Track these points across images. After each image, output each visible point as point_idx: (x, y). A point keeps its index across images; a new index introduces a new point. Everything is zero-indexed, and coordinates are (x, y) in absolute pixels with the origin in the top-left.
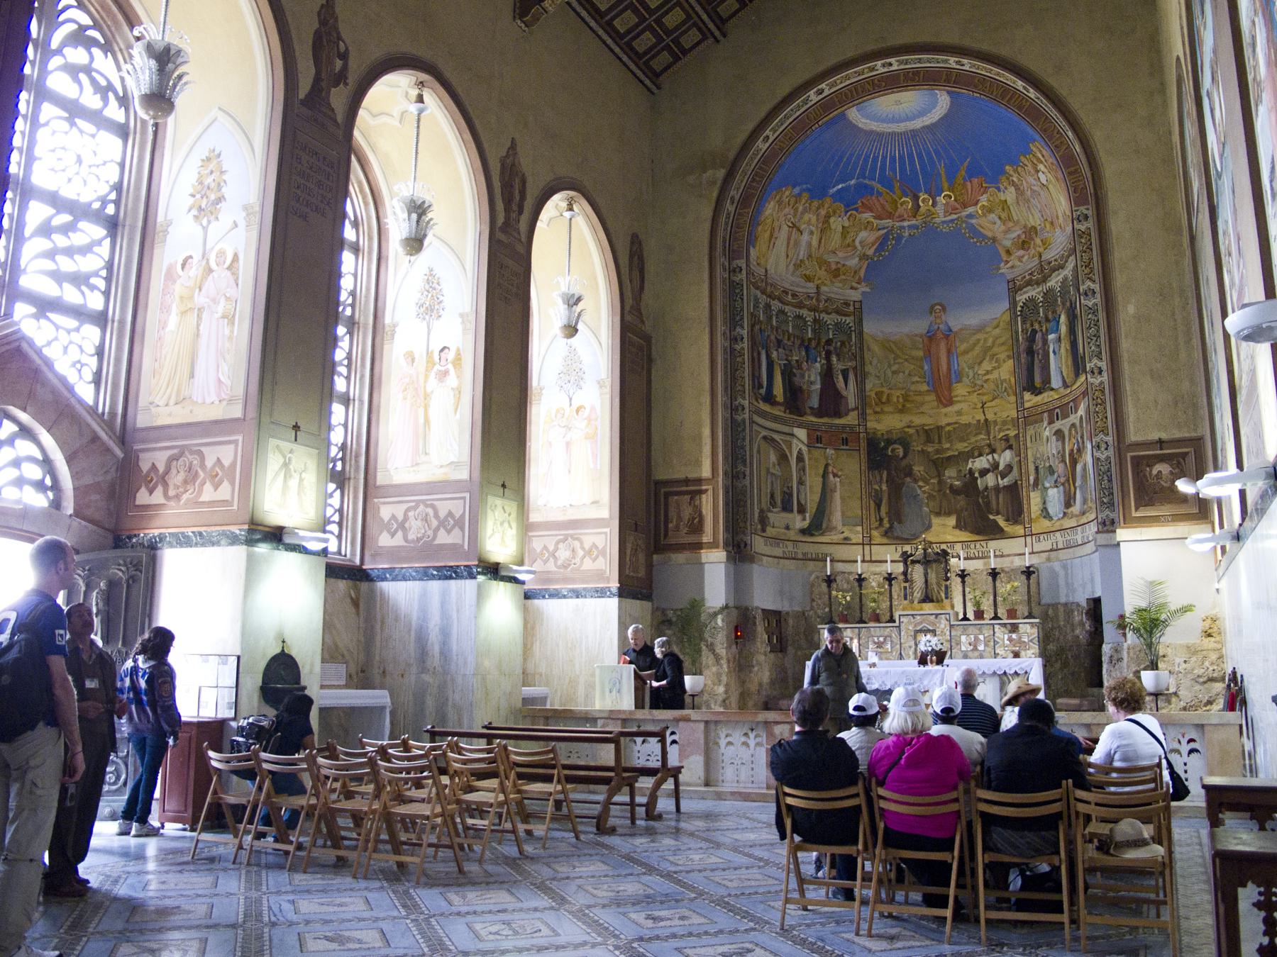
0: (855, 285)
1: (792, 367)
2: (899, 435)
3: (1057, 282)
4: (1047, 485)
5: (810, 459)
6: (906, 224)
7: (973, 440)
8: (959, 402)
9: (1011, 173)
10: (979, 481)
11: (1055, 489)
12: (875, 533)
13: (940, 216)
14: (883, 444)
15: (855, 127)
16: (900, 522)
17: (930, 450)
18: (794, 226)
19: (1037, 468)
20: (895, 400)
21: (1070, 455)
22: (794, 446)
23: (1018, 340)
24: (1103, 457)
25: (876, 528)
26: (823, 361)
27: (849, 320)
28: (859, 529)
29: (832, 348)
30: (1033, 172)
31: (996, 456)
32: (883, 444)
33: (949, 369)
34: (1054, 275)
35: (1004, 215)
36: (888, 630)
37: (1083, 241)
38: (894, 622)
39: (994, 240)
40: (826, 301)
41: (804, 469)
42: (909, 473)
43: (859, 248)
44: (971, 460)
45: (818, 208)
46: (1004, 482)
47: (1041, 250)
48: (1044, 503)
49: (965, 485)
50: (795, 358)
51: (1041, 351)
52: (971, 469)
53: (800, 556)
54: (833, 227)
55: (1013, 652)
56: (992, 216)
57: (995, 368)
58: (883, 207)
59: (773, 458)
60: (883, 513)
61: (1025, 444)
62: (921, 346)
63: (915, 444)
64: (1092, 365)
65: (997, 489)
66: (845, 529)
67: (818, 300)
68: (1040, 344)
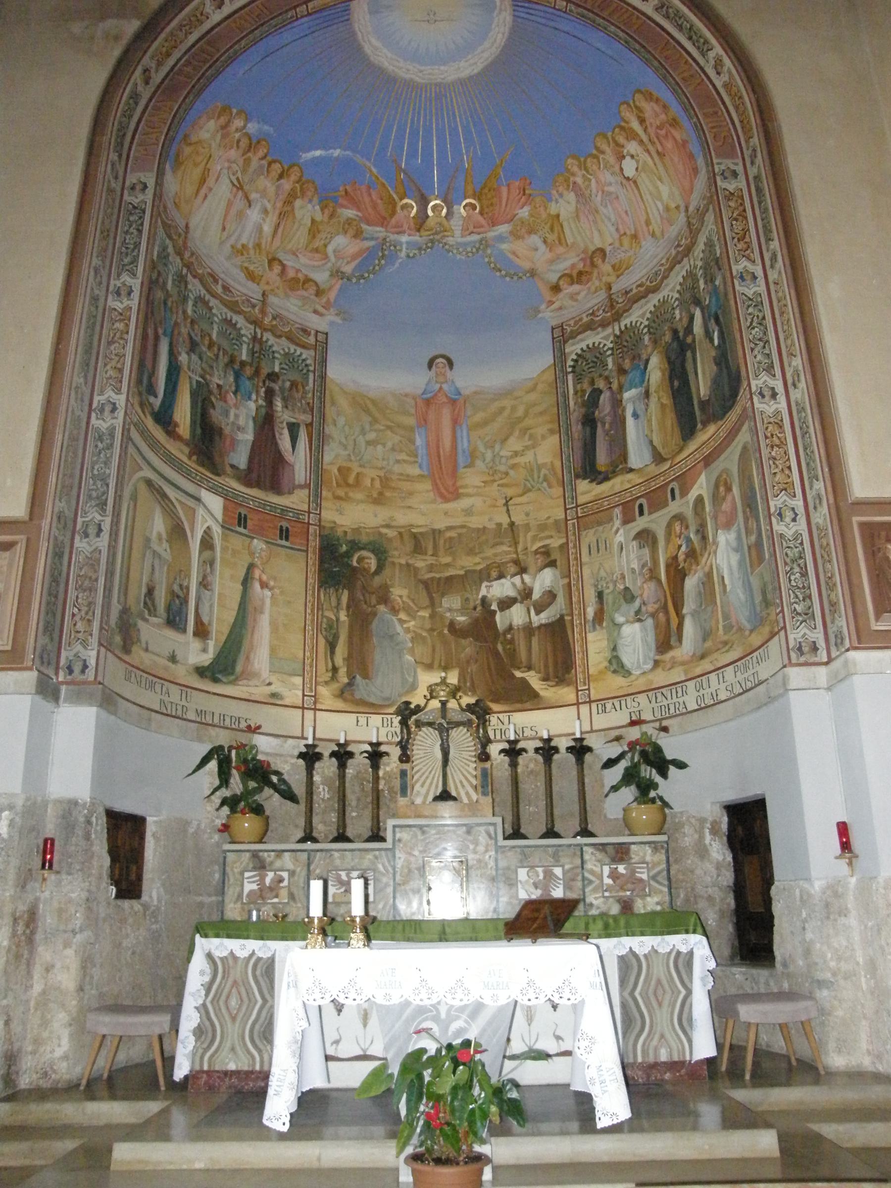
1: (210, 392)
2: (372, 539)
4: (620, 619)
5: (224, 549)
6: (404, 239)
7: (489, 552)
9: (575, 169)
10: (498, 617)
11: (637, 625)
12: (323, 691)
13: (456, 237)
15: (359, 49)
16: (366, 676)
18: (240, 188)
19: (600, 595)
20: (368, 482)
21: (668, 566)
22: (199, 518)
23: (567, 406)
24: (789, 533)
25: (326, 683)
26: (261, 402)
27: (307, 354)
28: (298, 680)
29: (276, 387)
30: (612, 160)
31: (525, 576)
32: (344, 548)
33: (454, 446)
34: (635, 306)
35: (551, 237)
36: (370, 856)
37: (732, 204)
38: (383, 840)
39: (533, 273)
40: (274, 318)
41: (212, 563)
42: (385, 599)
43: (333, 259)
44: (485, 584)
45: (281, 176)
46: (538, 620)
48: (614, 649)
49: (475, 623)
51: (608, 419)
53: (191, 716)
54: (298, 213)
55: (619, 900)
56: (535, 240)
57: (527, 448)
58: (375, 206)
59: (159, 525)
60: (339, 660)
61: (578, 558)
62: (413, 411)
63: (396, 553)
64: (760, 383)
65: (529, 630)
66: (273, 679)
67: (263, 312)
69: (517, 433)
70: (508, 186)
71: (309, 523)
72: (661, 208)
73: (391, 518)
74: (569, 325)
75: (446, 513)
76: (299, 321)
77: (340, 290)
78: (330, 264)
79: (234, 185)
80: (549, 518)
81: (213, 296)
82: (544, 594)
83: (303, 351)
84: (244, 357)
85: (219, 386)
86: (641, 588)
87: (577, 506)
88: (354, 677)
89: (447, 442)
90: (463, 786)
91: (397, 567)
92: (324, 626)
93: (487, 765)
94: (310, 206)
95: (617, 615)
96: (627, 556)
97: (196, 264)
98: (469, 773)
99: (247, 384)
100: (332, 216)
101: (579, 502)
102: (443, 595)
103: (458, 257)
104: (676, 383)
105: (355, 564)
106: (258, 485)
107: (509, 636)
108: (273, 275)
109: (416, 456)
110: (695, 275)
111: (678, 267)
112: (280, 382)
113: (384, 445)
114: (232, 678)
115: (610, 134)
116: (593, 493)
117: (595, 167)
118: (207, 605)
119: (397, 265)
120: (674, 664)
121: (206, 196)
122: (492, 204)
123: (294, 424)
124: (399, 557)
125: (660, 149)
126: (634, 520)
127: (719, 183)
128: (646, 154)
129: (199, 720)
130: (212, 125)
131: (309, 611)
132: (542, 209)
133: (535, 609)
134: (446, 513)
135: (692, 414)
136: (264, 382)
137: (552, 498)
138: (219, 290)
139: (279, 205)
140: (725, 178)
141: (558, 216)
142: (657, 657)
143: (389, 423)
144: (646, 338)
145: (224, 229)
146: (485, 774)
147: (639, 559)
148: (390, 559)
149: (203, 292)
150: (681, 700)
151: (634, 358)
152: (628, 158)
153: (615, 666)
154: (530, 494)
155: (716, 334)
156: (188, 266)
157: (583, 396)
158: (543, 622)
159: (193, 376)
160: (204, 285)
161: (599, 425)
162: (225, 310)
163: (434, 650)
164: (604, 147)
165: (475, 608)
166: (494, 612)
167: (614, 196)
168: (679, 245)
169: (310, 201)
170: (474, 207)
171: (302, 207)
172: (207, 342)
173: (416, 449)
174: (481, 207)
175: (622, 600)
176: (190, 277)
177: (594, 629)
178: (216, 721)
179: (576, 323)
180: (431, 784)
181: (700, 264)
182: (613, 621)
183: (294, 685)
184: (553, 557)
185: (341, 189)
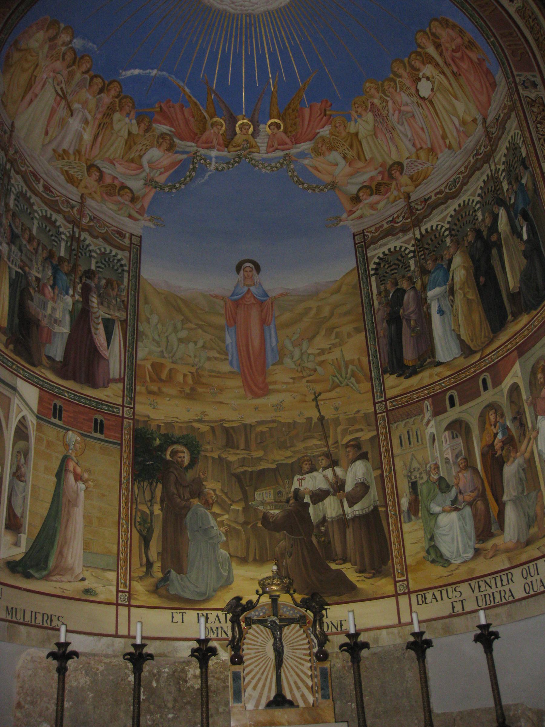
0: (136, 215)
1: (28, 284)
2: (185, 433)
3: (443, 220)
4: (436, 509)
5: (39, 440)
6: (214, 153)
7: (300, 446)
8: (278, 391)
10: (311, 510)
11: (454, 515)
12: (138, 587)
14: (158, 442)
16: (180, 571)
17: (232, 458)
18: (64, 97)
19: (414, 486)
20: (180, 379)
21: (483, 455)
25: (141, 578)
26: (77, 297)
28: (112, 576)
30: (408, 82)
31: (338, 470)
32: (158, 442)
34: (435, 212)
35: (350, 154)
39: (333, 186)
40: (91, 219)
41: (26, 453)
43: (147, 170)
44: (297, 477)
45: (101, 91)
46: (351, 511)
47: (410, 188)
48: (432, 538)
50: (34, 273)
51: (413, 317)
52: (297, 491)
54: (116, 127)
56: (335, 156)
57: (334, 345)
58: (187, 121)
62: (223, 312)
63: (208, 447)
66: (87, 574)
67: (81, 212)
68: (412, 307)
69: (323, 333)
70: (311, 107)
71: (123, 417)
72: (457, 123)
73: (204, 413)
74: (371, 232)
75: (256, 408)
76: (114, 224)
77: (154, 198)
78: (144, 174)
79: (58, 94)
80: (358, 412)
81: (36, 195)
82: (357, 485)
83: (119, 252)
84: (62, 254)
85: (37, 279)
86: (457, 477)
87: (386, 400)
88: (169, 572)
89: (257, 342)
90: (298, 688)
91: (210, 461)
92: (138, 519)
93: (327, 665)
94: (127, 120)
95: (432, 505)
96: (441, 445)
97: (19, 161)
98: (305, 674)
99: (63, 279)
100: (147, 130)
101: (388, 396)
102: (256, 489)
103: (264, 170)
104: (482, 279)
105: (168, 457)
106: (74, 378)
107: (323, 528)
108: (91, 181)
109: (227, 355)
110: (498, 178)
111: (477, 173)
112: (96, 280)
113: (196, 343)
114: (45, 573)
115: (406, 60)
116: (401, 387)
117: (391, 90)
118: (20, 497)
119: (206, 177)
120: (496, 551)
121: (31, 101)
122: (295, 124)
123: (108, 320)
124: (212, 451)
125: (455, 70)
126: (445, 411)
127: (521, 91)
128: (442, 76)
129: (9, 618)
130: (41, 35)
131: (123, 504)
132: (342, 127)
133: (348, 500)
134: (256, 408)
135: (502, 306)
136: (81, 278)
137: (360, 393)
138: (40, 188)
139: (99, 116)
140: (527, 88)
141: (357, 134)
142: (478, 546)
143: (200, 323)
144: (448, 240)
145: (47, 133)
146: (324, 674)
147: (453, 450)
148: (202, 453)
149: (25, 188)
150: (506, 588)
151: (436, 259)
152: (424, 80)
153: (433, 556)
154: (338, 389)
155: (524, 229)
156: (12, 162)
157: (387, 296)
158: (357, 513)
159: (13, 266)
160: (25, 181)
161: (404, 323)
162: (46, 208)
163: (248, 542)
164: (401, 71)
165: (288, 501)
166: (308, 504)
167: (409, 115)
168: (478, 154)
169: (128, 115)
170: (278, 126)
171: (119, 121)
172: (27, 236)
173: (227, 346)
174: (286, 127)
175: (437, 490)
176: (12, 173)
177: (410, 520)
178: (27, 619)
179: (377, 230)
180: (264, 686)
181: (502, 167)
182: (428, 510)
183: (108, 580)
184: (364, 449)
185: (157, 106)
